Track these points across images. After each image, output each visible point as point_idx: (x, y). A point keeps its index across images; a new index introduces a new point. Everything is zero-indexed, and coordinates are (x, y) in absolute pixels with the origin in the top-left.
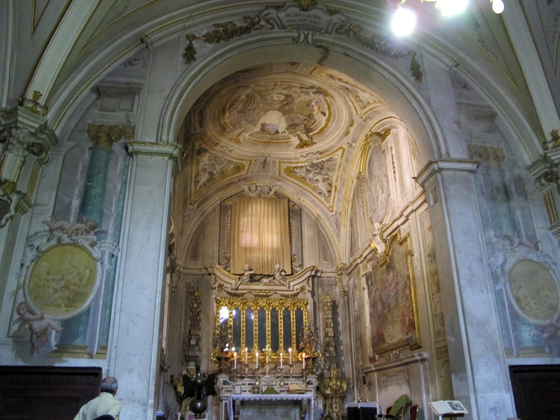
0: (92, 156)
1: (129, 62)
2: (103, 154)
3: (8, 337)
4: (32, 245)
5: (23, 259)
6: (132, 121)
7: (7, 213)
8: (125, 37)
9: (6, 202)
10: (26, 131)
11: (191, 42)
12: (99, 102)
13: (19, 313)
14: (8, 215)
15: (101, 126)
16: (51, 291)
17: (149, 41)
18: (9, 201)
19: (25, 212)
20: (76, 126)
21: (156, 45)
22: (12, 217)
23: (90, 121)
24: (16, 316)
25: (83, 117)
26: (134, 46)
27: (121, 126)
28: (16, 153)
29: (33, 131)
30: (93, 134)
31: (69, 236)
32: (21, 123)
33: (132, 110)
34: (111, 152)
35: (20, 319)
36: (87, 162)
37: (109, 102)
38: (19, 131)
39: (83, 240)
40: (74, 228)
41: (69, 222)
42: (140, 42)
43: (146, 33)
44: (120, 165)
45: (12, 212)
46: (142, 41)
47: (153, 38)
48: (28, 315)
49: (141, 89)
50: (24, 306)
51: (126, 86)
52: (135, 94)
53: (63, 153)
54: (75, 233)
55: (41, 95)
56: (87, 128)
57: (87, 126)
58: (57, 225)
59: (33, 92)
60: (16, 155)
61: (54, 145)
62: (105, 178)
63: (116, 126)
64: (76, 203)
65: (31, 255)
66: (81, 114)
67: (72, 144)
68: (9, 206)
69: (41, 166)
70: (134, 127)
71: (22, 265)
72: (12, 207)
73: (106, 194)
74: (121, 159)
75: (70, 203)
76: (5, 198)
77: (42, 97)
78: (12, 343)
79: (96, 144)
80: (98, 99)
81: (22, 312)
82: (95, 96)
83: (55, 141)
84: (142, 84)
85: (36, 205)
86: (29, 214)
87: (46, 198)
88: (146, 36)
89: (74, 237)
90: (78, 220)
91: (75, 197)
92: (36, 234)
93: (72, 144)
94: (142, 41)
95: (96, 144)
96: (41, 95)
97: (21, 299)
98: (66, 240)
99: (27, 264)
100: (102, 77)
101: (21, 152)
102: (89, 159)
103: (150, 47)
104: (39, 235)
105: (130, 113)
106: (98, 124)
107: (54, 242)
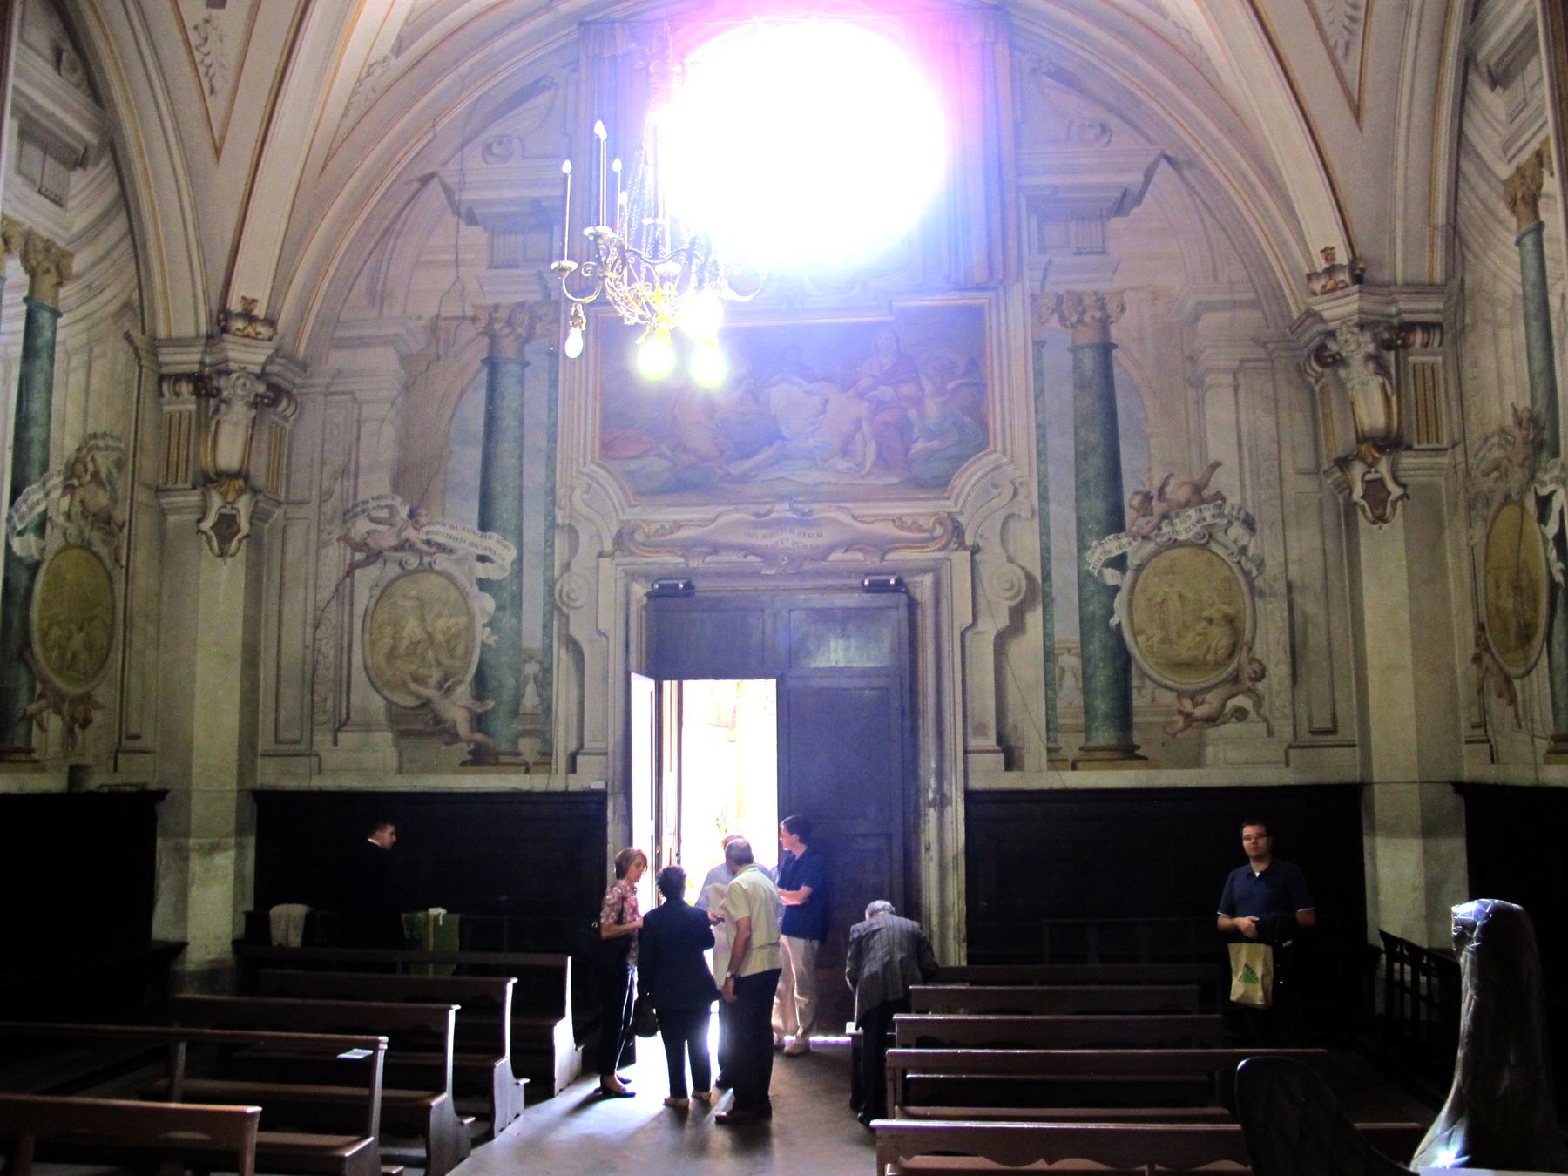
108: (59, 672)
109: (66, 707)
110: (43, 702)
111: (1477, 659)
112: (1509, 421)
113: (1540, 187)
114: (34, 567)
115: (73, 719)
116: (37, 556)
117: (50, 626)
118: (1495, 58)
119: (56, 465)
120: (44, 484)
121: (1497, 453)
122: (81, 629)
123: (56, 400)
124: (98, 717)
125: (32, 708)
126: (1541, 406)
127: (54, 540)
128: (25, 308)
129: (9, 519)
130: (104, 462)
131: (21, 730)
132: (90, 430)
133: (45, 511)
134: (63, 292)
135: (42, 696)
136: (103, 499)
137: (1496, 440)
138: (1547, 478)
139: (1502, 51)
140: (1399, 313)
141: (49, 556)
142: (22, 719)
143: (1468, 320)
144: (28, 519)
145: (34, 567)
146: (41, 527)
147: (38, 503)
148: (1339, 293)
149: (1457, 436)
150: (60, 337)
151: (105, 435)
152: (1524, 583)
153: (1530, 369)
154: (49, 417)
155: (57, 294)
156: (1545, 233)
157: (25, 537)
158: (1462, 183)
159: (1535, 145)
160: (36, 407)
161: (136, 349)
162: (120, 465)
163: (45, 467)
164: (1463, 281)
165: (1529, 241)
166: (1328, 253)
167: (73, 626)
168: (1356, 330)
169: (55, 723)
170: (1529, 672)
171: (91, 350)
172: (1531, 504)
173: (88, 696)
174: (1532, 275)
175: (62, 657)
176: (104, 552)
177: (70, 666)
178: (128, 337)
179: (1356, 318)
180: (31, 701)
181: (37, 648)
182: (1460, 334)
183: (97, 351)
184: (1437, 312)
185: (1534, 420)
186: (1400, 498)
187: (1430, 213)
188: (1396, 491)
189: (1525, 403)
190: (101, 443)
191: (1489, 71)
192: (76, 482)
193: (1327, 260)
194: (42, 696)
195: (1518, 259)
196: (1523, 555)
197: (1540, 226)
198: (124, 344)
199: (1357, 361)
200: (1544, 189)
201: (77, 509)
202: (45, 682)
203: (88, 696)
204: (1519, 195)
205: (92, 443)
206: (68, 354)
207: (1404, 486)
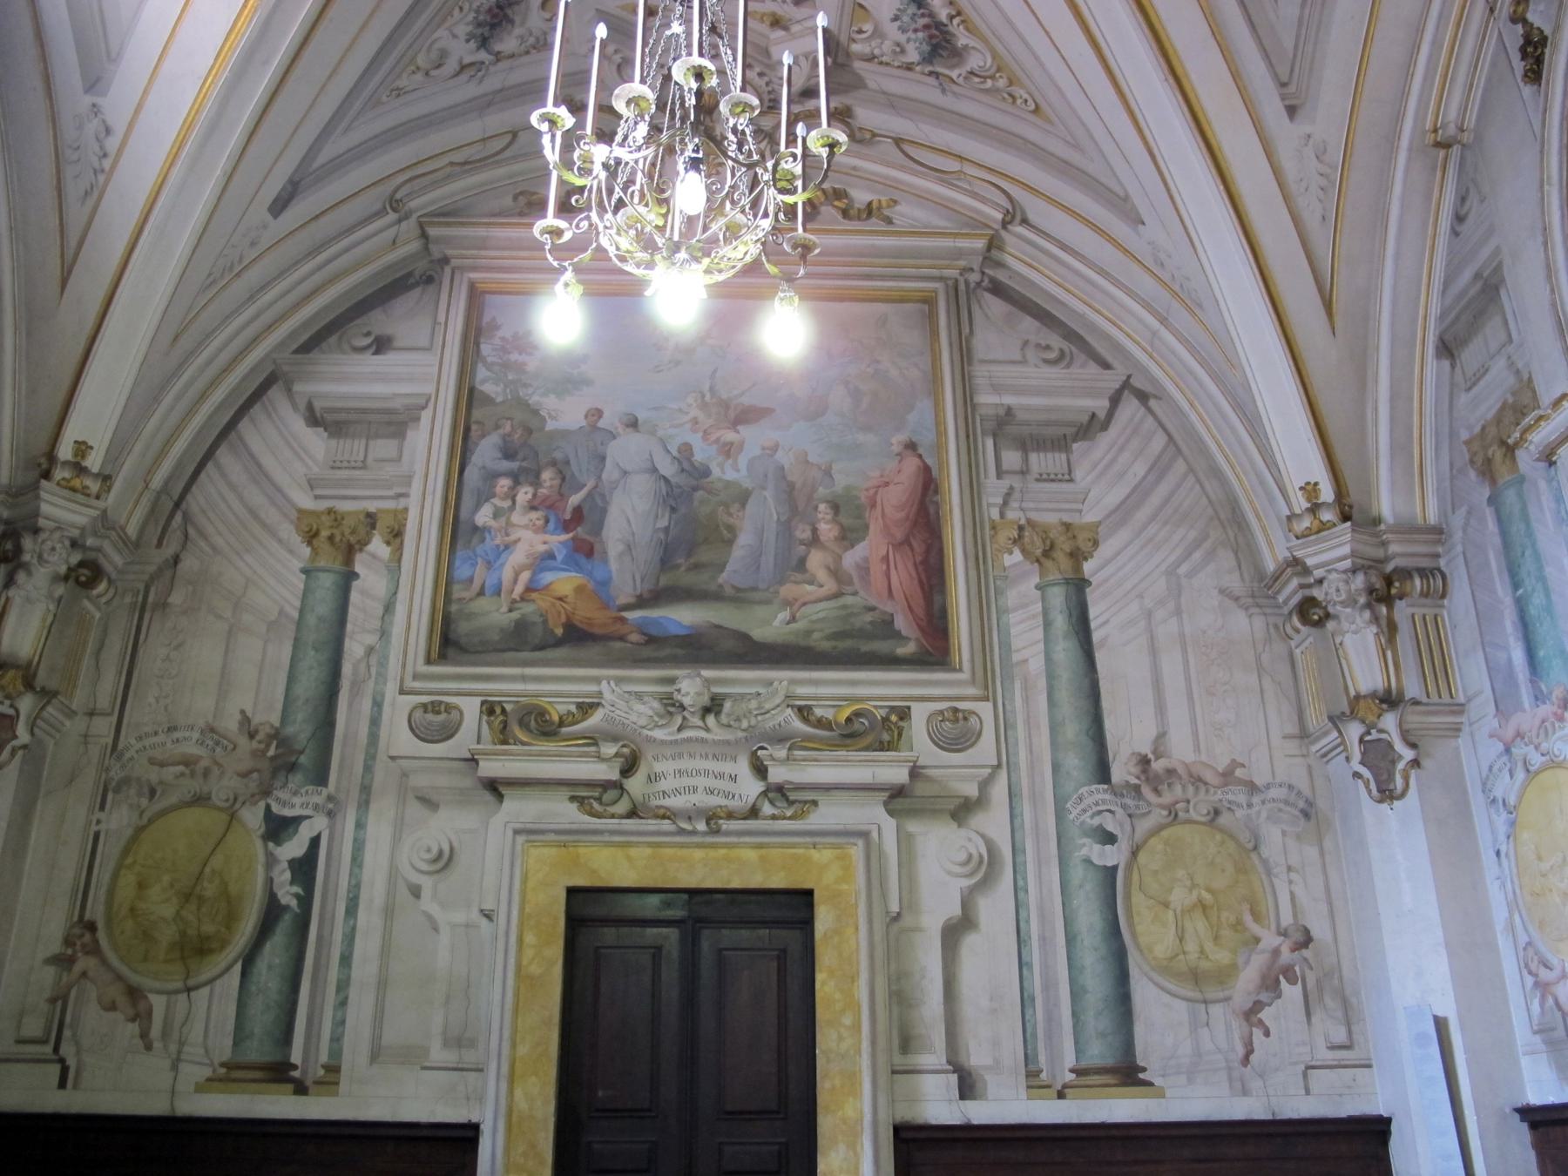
0: (1499, 520)
1: (1459, 218)
2: (1510, 496)
3: (1535, 1033)
4: (1494, 801)
5: (1495, 840)
6: (1520, 365)
7: (1393, 762)
8: (1398, 189)
9: (1379, 740)
10: (1334, 576)
11: (1524, 21)
12: (1458, 369)
13: (1530, 973)
14: (1401, 766)
15: (1483, 428)
16: (1558, 900)
17: (1452, 130)
18: (1383, 736)
19: (1459, 730)
20: (1452, 465)
21: (1471, 121)
22: (1415, 763)
23: (1464, 435)
24: (1529, 981)
25: (1453, 434)
26: (1439, 174)
27: (1510, 400)
28: (1353, 627)
29: (1347, 563)
30: (1479, 459)
31: (1536, 748)
32: (1317, 567)
33: (1510, 340)
34: (1522, 480)
35: (1536, 984)
36: (1497, 540)
37: (1470, 356)
38: (1325, 584)
39: (1559, 745)
40: (1537, 722)
41: (1524, 711)
42: (1442, 153)
43: (1429, 125)
44: (1547, 501)
45: (1408, 754)
46: (1445, 145)
47: (1453, 114)
48: (1545, 974)
49: (1499, 267)
50: (1531, 952)
51: (1479, 285)
52: (1497, 289)
53: (1459, 548)
54: (1542, 735)
55: (1316, 484)
56: (1467, 457)
57: (1464, 448)
58: (1509, 733)
59: (1300, 494)
60: (1355, 633)
61: (1439, 542)
62: (1537, 557)
63: (1505, 404)
64: (1518, 655)
65: (1501, 820)
66: (1446, 430)
67: (1462, 511)
68: (1390, 745)
69: (1442, 606)
70: (1530, 380)
71: (1498, 853)
72: (1399, 746)
73: (1554, 597)
74: (1542, 484)
75: (1510, 660)
76: (1374, 735)
77: (1320, 486)
78: (1543, 1047)
79: (1493, 481)
80: (1453, 366)
81: (1533, 967)
82: (1446, 364)
83: (1438, 533)
84: (1497, 251)
85: (1469, 700)
86: (1466, 729)
87: (1471, 675)
88: (1435, 131)
89: (1544, 746)
90: (1537, 698)
91: (1512, 640)
92: (1491, 768)
93: (1462, 511)
94: (1445, 145)
95: (1493, 481)
96: (1316, 484)
97: (1523, 939)
98: (1536, 760)
99: (1503, 849)
100: (1435, 310)
101: (1358, 620)
102: (1496, 530)
103: (1467, 137)
104: (1495, 769)
105: (1510, 349)
106: (1477, 429)
107: (1520, 775)
111: (63, 961)
112: (231, 724)
113: (364, 543)
118: (328, 404)
121: (192, 749)
126: (301, 729)
137: (196, 735)
138: (297, 800)
139: (339, 404)
140: (99, 550)
143: (176, 598)
148: (80, 497)
149: (103, 702)
152: (210, 889)
153: (288, 689)
156: (355, 584)
158: (210, 465)
159: (372, 507)
164: (176, 560)
165: (327, 581)
166: (82, 448)
168: (67, 543)
170: (189, 990)
172: (253, 817)
174: (323, 606)
179: (75, 533)
182: (146, 609)
184: (116, 568)
185: (276, 736)
186: (24, 747)
187: (151, 471)
188: (23, 735)
189: (269, 716)
191: (310, 407)
193: (76, 455)
195: (302, 586)
196: (217, 862)
197: (350, 576)
199: (42, 575)
200: (371, 548)
204: (325, 533)
207: (32, 734)
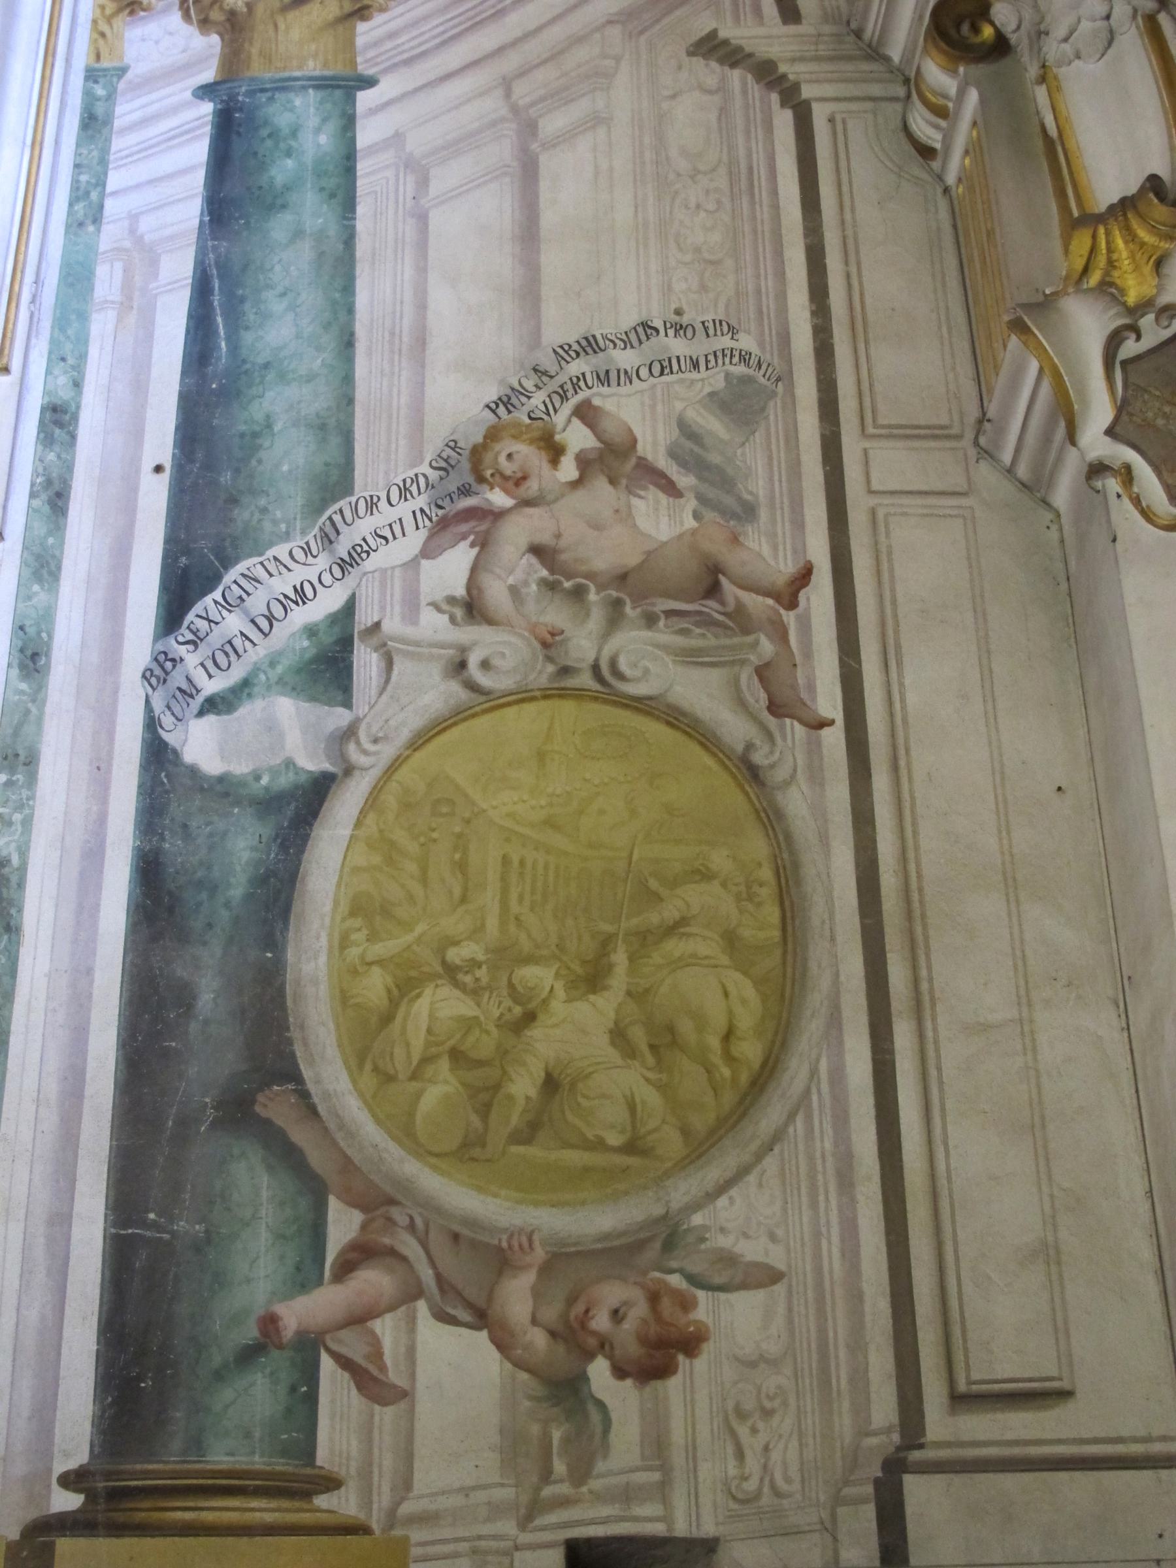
108: (466, 1154)
109: (517, 1298)
110: (373, 1280)
114: (301, 805)
115: (575, 1338)
116: (312, 763)
117: (406, 986)
119: (386, 459)
120: (328, 539)
122: (591, 979)
123: (376, 293)
124: (736, 1321)
125: (298, 1313)
127: (397, 699)
128: (207, 108)
129: (161, 668)
130: (643, 415)
131: (253, 1400)
132: (560, 328)
133: (350, 608)
134: (365, 32)
135: (360, 1254)
136: (660, 523)
141: (370, 759)
142: (249, 1355)
144: (255, 654)
145: (301, 805)
146: (328, 667)
147: (300, 596)
150: (365, 136)
151: (647, 328)
154: (348, 343)
155: (348, 45)
157: (250, 711)
160: (281, 327)
161: (767, 73)
162: (742, 403)
163: (334, 483)
167: (539, 977)
169: (454, 1371)
171: (529, 128)
173: (669, 1235)
175: (485, 1097)
176: (701, 692)
177: (528, 1133)
178: (712, 47)
180: (305, 1278)
181: (329, 1073)
183: (553, 123)
190: (625, 359)
192: (499, 498)
194: (360, 1254)
198: (709, 72)
201: (514, 569)
202: (376, 1201)
203: (669, 1235)
205: (576, 367)
206: (419, 171)
